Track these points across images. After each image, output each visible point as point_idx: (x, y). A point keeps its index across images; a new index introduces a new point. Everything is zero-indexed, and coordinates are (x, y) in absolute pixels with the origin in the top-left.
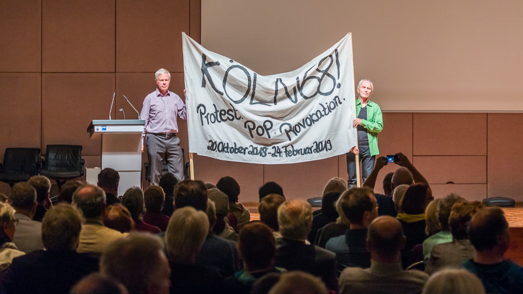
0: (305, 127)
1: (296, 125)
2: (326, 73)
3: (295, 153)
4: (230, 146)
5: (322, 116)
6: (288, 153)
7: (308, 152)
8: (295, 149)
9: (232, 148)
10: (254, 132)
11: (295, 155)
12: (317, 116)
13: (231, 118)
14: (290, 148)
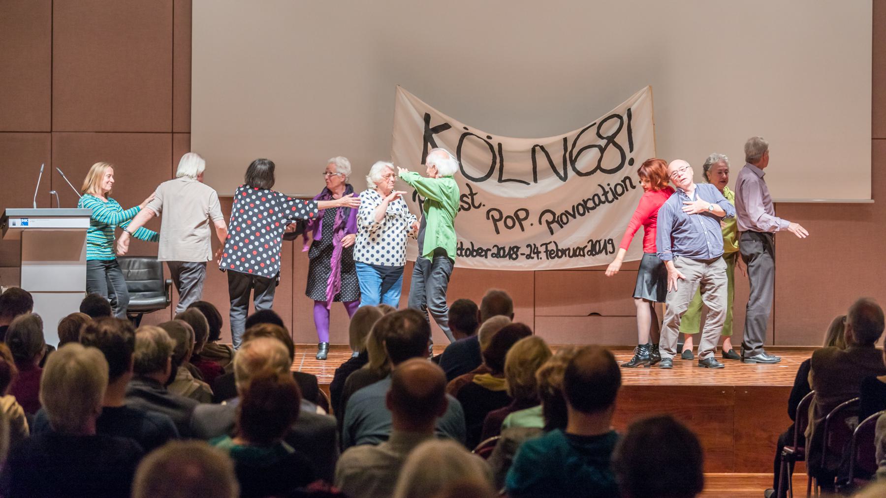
0: (575, 217)
1: (562, 214)
2: (611, 140)
3: (560, 254)
4: (465, 247)
5: (601, 202)
6: (550, 254)
7: (580, 255)
8: (560, 248)
9: (468, 249)
10: (501, 224)
11: (561, 257)
12: (594, 202)
13: (466, 206)
14: (552, 247)
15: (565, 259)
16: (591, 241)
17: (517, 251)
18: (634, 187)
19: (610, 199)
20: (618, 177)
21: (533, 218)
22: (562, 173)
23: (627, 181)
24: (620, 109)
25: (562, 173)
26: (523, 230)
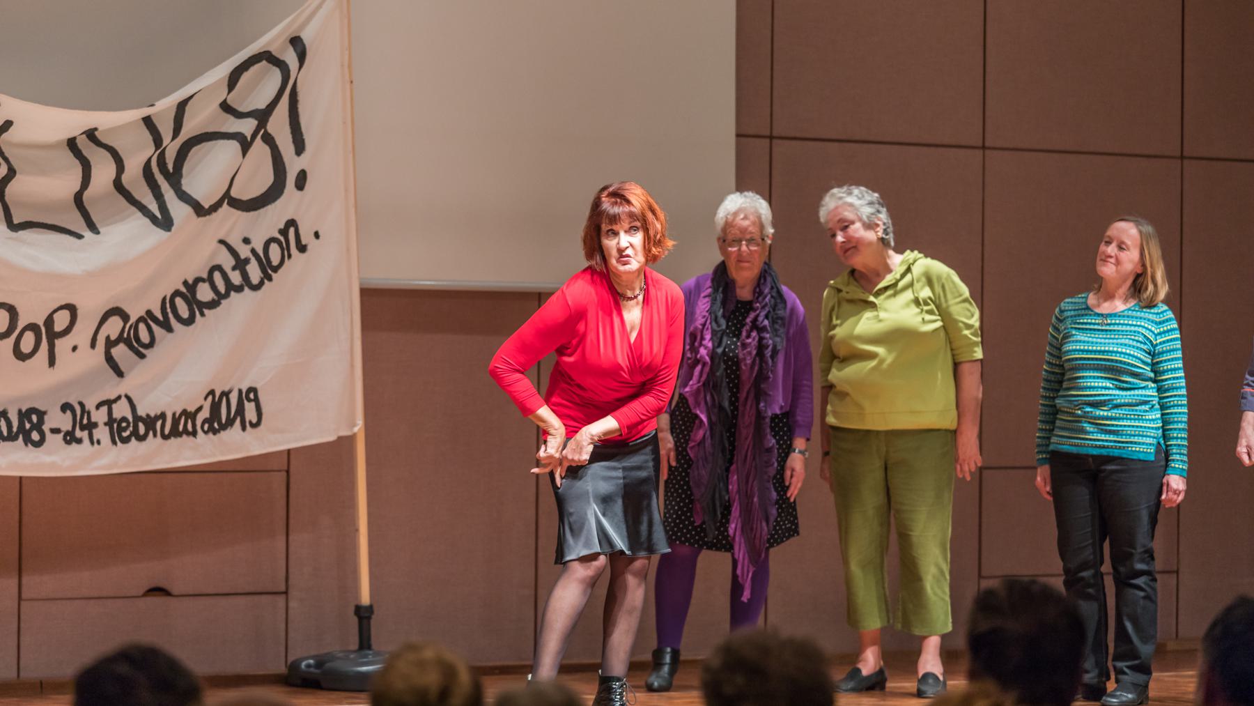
0: (169, 329)
5: (231, 287)
6: (121, 431)
7: (186, 432)
8: (141, 412)
12: (214, 287)
15: (153, 442)
16: (212, 392)
17: (41, 421)
18: (302, 248)
19: (255, 281)
20: (268, 222)
21: (82, 334)
22: (154, 207)
23: (292, 230)
24: (272, 39)
25: (154, 207)
26: (52, 362)
